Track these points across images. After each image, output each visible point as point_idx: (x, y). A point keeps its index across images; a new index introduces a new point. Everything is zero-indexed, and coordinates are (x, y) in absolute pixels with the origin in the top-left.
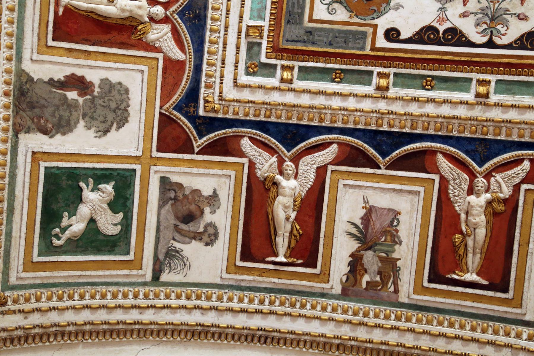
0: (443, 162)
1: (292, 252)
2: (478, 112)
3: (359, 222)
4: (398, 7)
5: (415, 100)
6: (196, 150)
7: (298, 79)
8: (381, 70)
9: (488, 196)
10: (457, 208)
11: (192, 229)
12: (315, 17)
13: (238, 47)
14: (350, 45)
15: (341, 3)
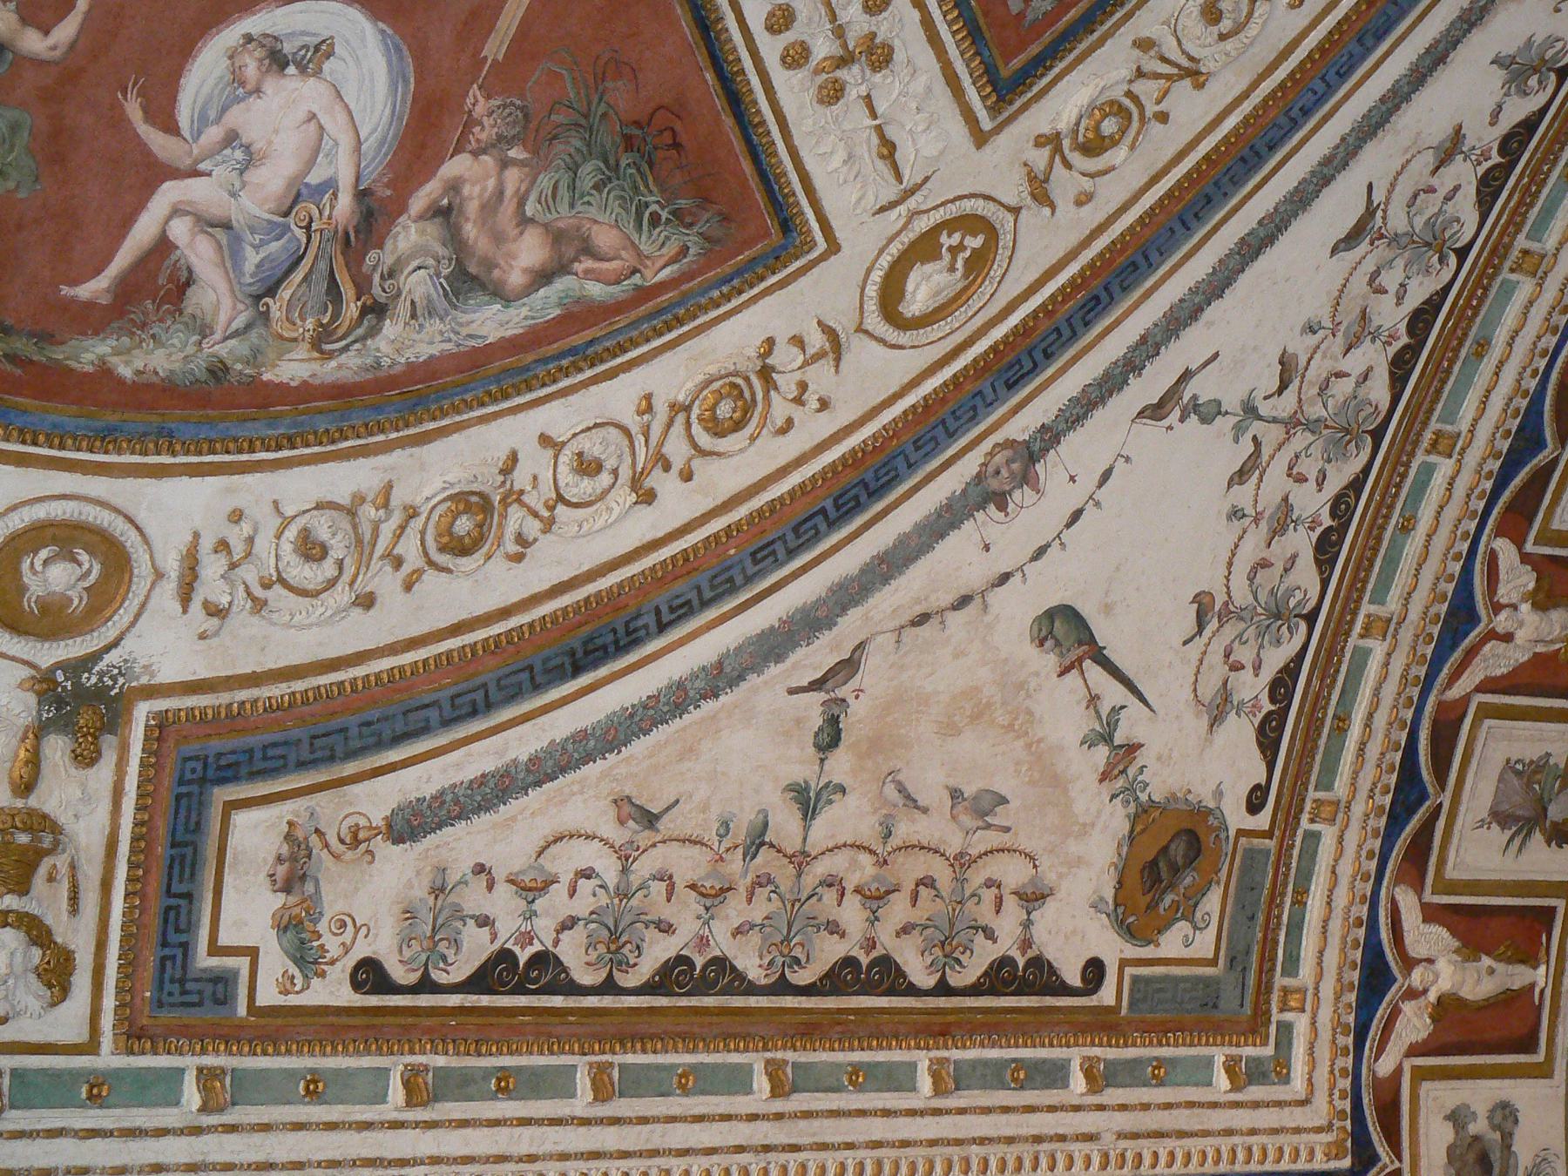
0: (1455, 692)
1: (1529, 958)
2: (1406, 635)
3: (1508, 833)
4: (1219, 794)
5: (1361, 749)
6: (1397, 1164)
7: (1297, 975)
8: (1305, 818)
9: (1525, 608)
10: (1526, 658)
11: (1498, 1154)
12: (1211, 955)
13: (1256, 1105)
14: (1258, 879)
15: (1196, 905)
